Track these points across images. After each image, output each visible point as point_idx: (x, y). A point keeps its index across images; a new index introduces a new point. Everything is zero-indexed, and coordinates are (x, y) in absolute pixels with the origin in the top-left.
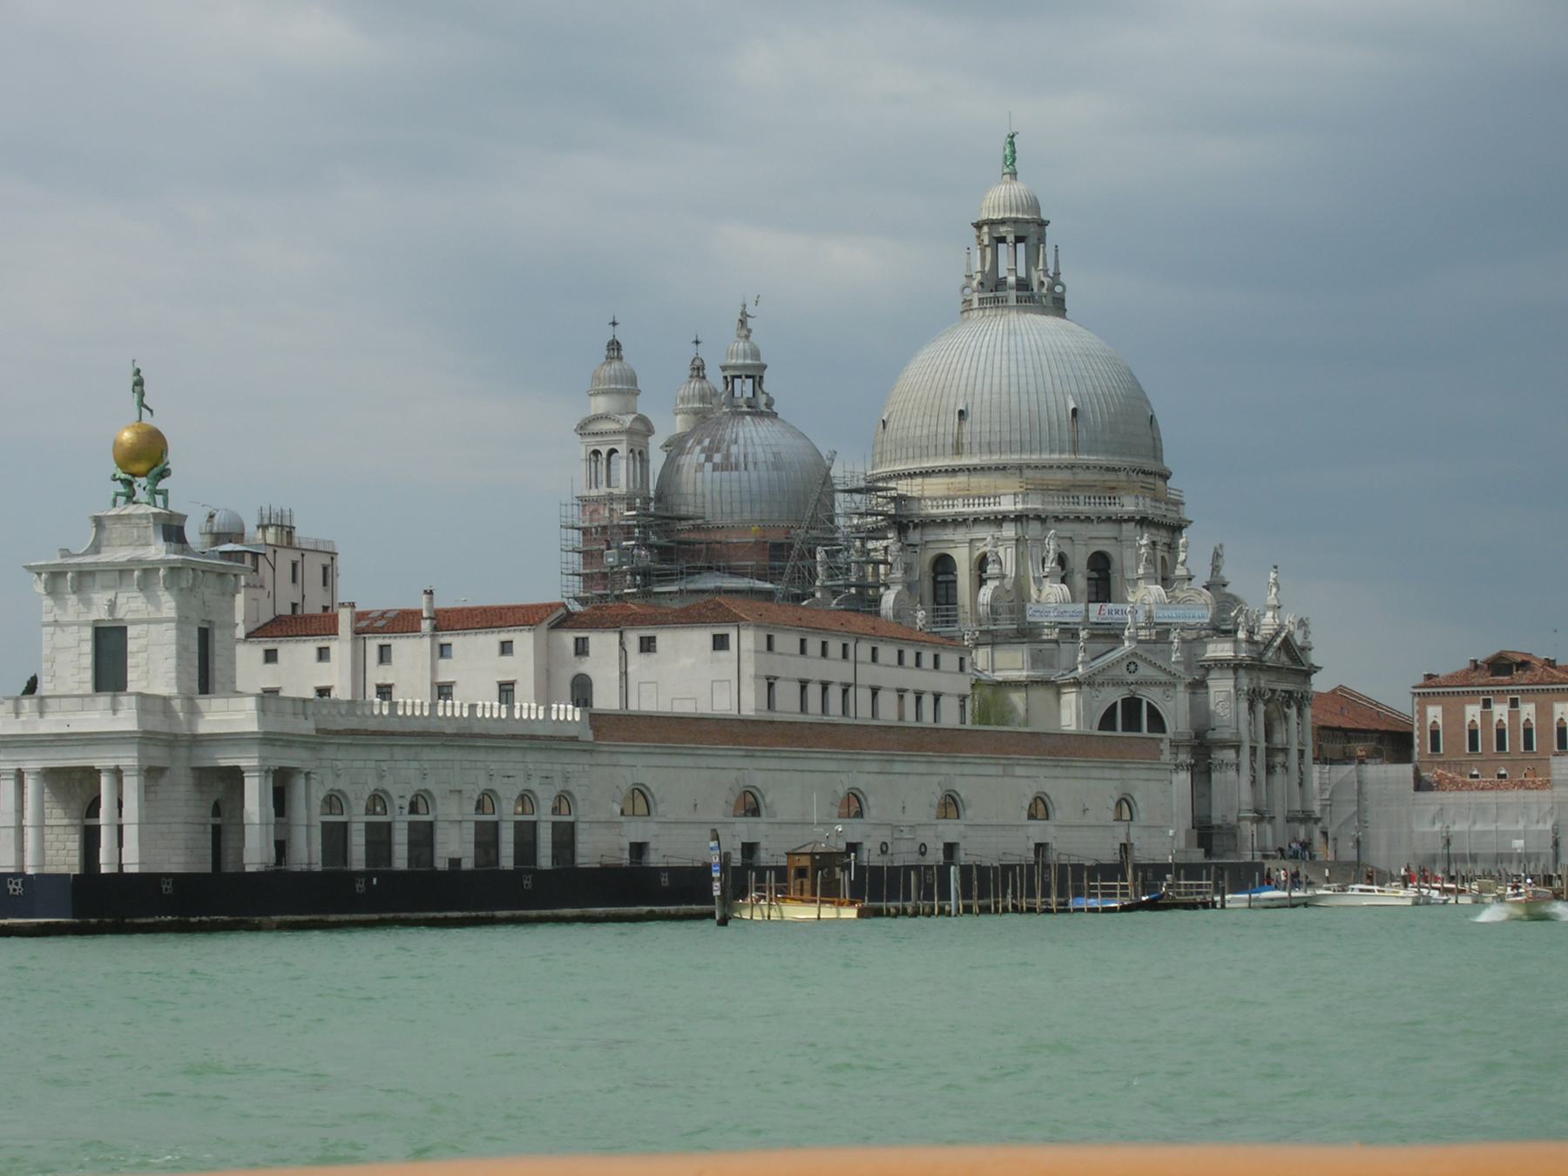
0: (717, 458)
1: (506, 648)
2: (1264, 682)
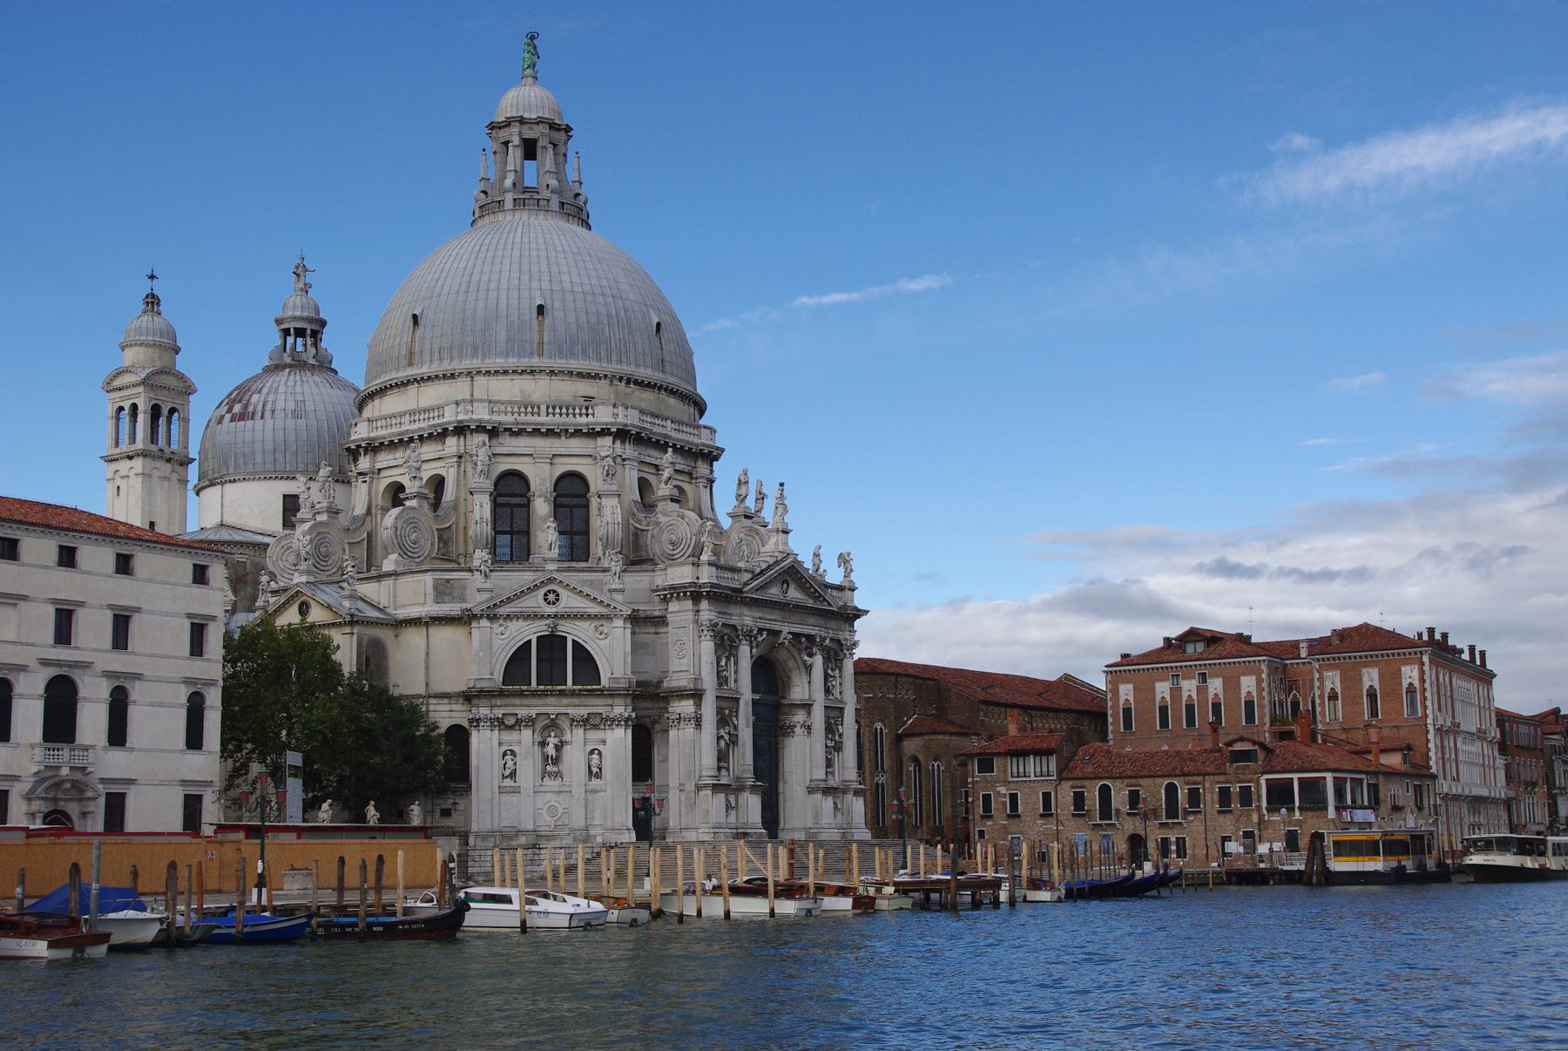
0: (237, 408)
2: (746, 618)
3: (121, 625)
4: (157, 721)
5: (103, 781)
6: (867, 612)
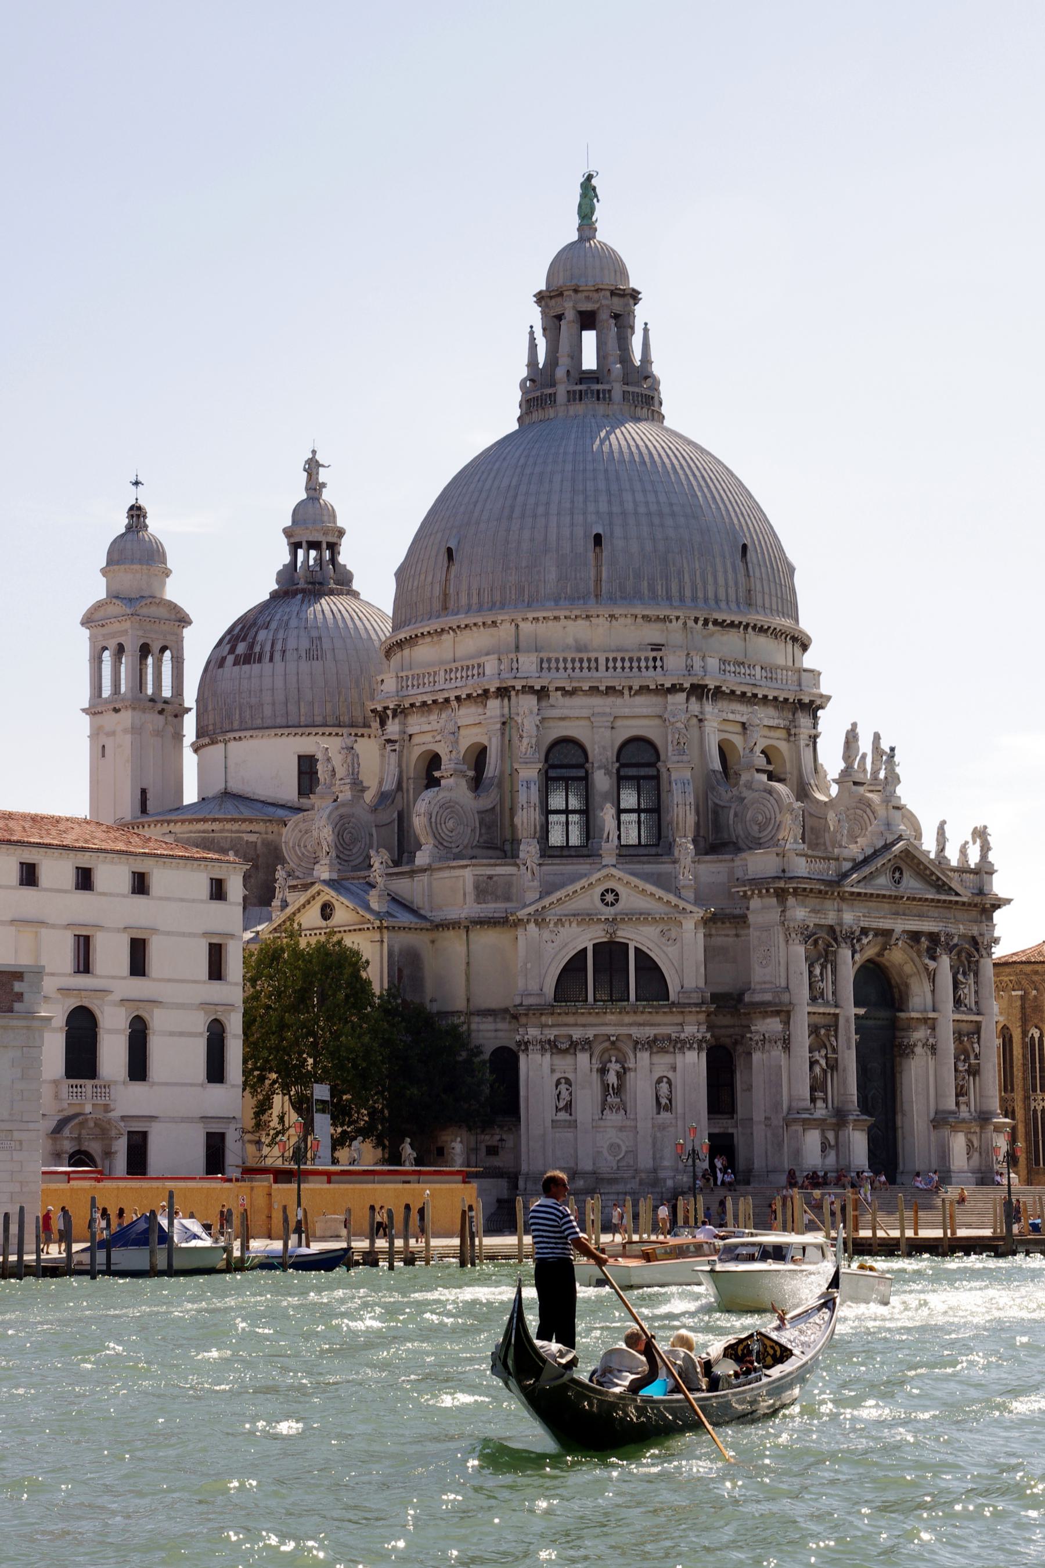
0: (241, 648)
3: (138, 950)
4: (177, 1054)
5: (123, 1118)
6: (1008, 901)
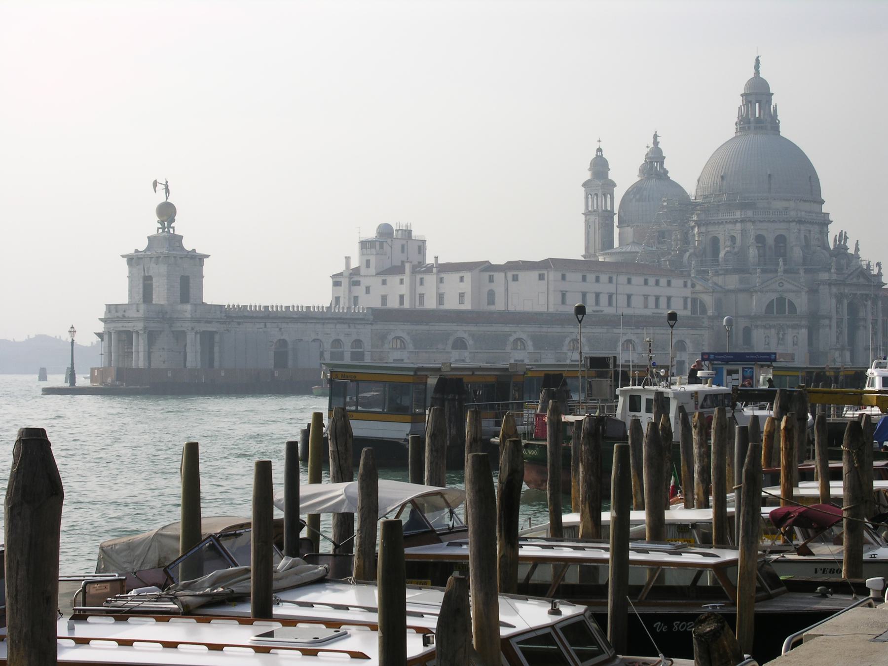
1: (462, 279)
